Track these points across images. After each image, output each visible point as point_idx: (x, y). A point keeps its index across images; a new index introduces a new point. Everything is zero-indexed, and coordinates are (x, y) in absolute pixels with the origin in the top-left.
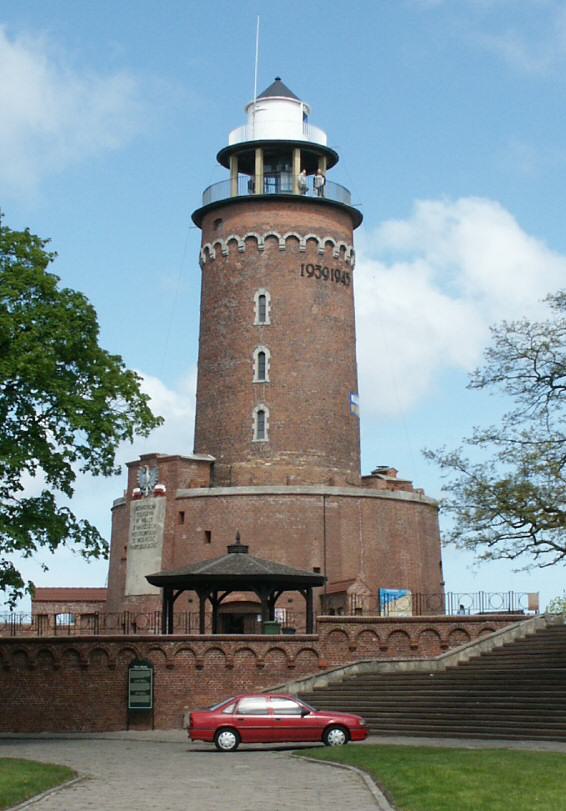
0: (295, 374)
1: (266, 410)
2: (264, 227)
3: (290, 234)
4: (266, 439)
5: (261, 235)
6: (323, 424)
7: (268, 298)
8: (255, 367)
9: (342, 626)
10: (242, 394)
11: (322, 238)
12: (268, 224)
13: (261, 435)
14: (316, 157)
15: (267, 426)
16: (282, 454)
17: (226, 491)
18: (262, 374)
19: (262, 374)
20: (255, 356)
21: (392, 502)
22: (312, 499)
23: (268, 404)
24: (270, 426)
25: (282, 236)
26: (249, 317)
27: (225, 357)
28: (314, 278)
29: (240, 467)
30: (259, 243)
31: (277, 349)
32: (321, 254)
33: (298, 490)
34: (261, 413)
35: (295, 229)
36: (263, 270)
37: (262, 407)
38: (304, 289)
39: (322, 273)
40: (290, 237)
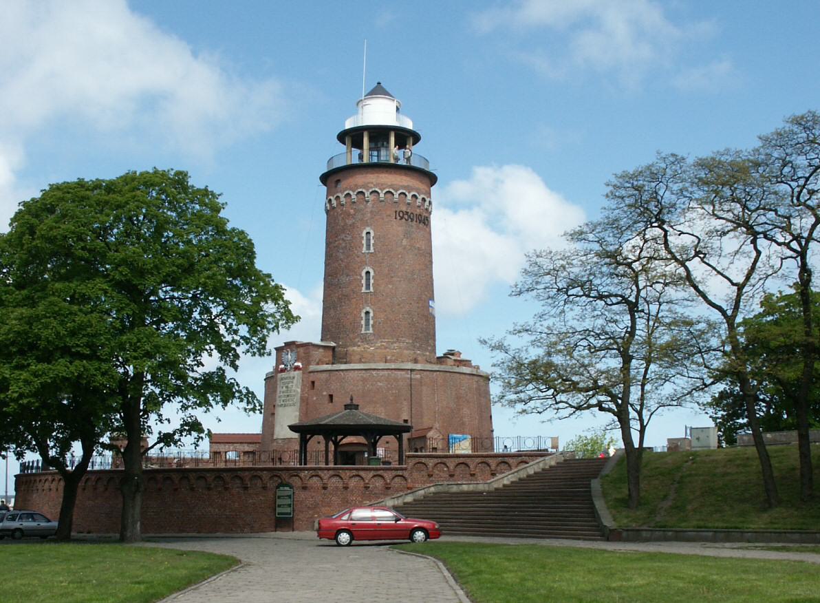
0: (390, 286)
1: (371, 311)
3: (387, 190)
4: (371, 331)
6: (410, 321)
7: (372, 234)
8: (364, 282)
9: (423, 460)
10: (355, 300)
11: (409, 192)
12: (372, 183)
13: (367, 329)
14: (405, 137)
15: (371, 322)
16: (382, 342)
17: (343, 367)
18: (368, 287)
19: (368, 287)
20: (363, 274)
21: (458, 375)
22: (403, 373)
23: (372, 307)
24: (375, 323)
25: (382, 191)
27: (343, 274)
28: (404, 220)
29: (353, 350)
30: (366, 196)
31: (379, 269)
32: (409, 204)
33: (393, 366)
34: (367, 313)
35: (391, 186)
37: (368, 309)
38: (397, 228)
39: (410, 217)
40: (387, 192)
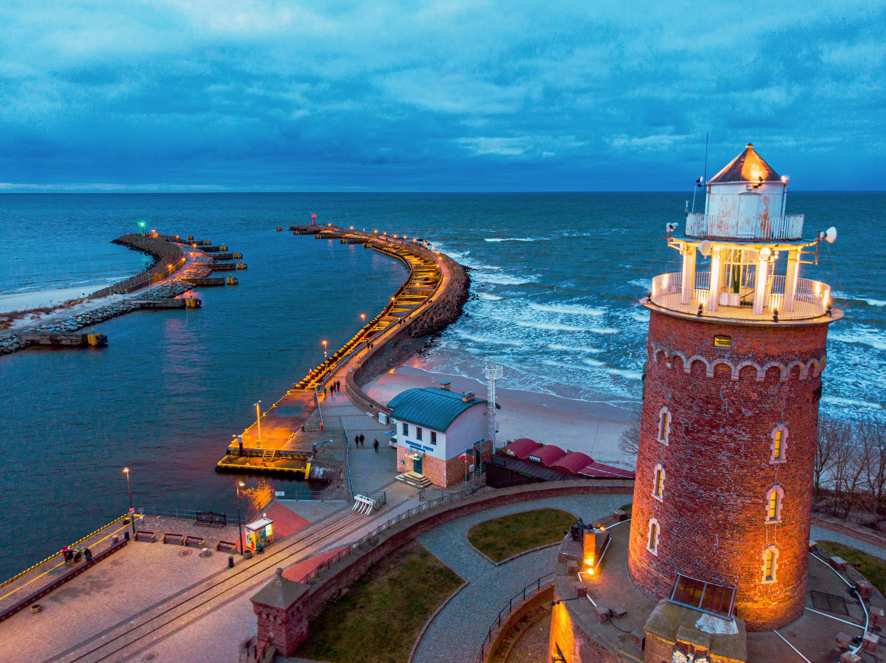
5: (786, 365)
26: (765, 455)
31: (790, 487)
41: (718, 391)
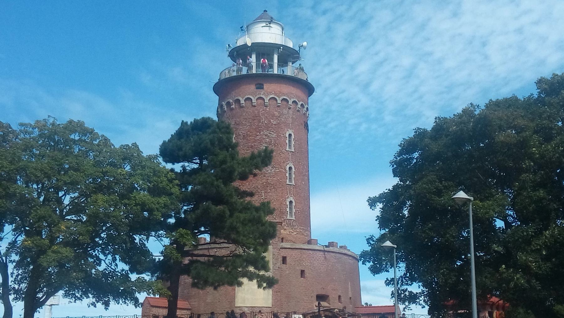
2: (292, 95)
7: (293, 137)
10: (281, 189)
13: (291, 216)
19: (290, 181)
36: (291, 120)
37: (292, 199)
41: (259, 113)
